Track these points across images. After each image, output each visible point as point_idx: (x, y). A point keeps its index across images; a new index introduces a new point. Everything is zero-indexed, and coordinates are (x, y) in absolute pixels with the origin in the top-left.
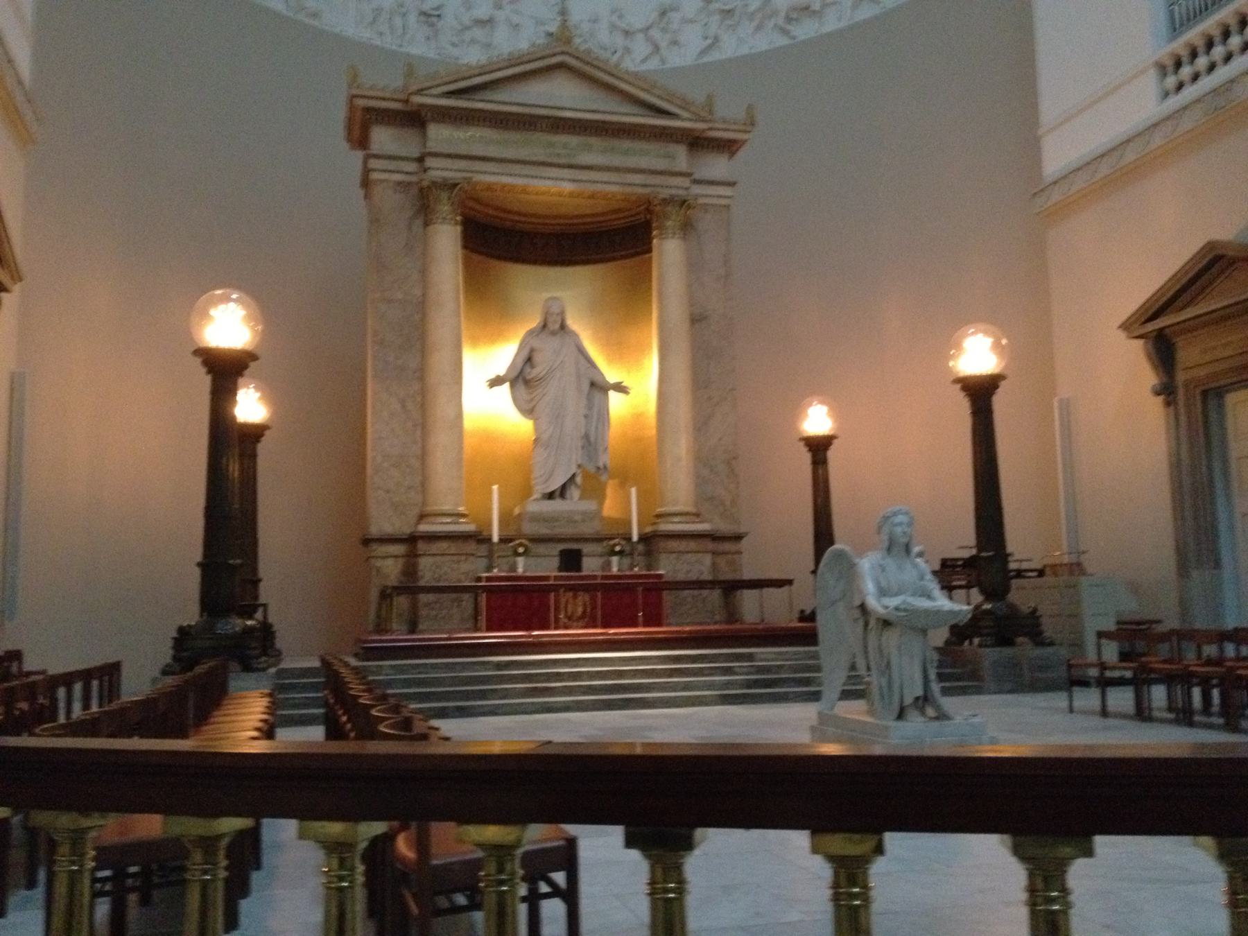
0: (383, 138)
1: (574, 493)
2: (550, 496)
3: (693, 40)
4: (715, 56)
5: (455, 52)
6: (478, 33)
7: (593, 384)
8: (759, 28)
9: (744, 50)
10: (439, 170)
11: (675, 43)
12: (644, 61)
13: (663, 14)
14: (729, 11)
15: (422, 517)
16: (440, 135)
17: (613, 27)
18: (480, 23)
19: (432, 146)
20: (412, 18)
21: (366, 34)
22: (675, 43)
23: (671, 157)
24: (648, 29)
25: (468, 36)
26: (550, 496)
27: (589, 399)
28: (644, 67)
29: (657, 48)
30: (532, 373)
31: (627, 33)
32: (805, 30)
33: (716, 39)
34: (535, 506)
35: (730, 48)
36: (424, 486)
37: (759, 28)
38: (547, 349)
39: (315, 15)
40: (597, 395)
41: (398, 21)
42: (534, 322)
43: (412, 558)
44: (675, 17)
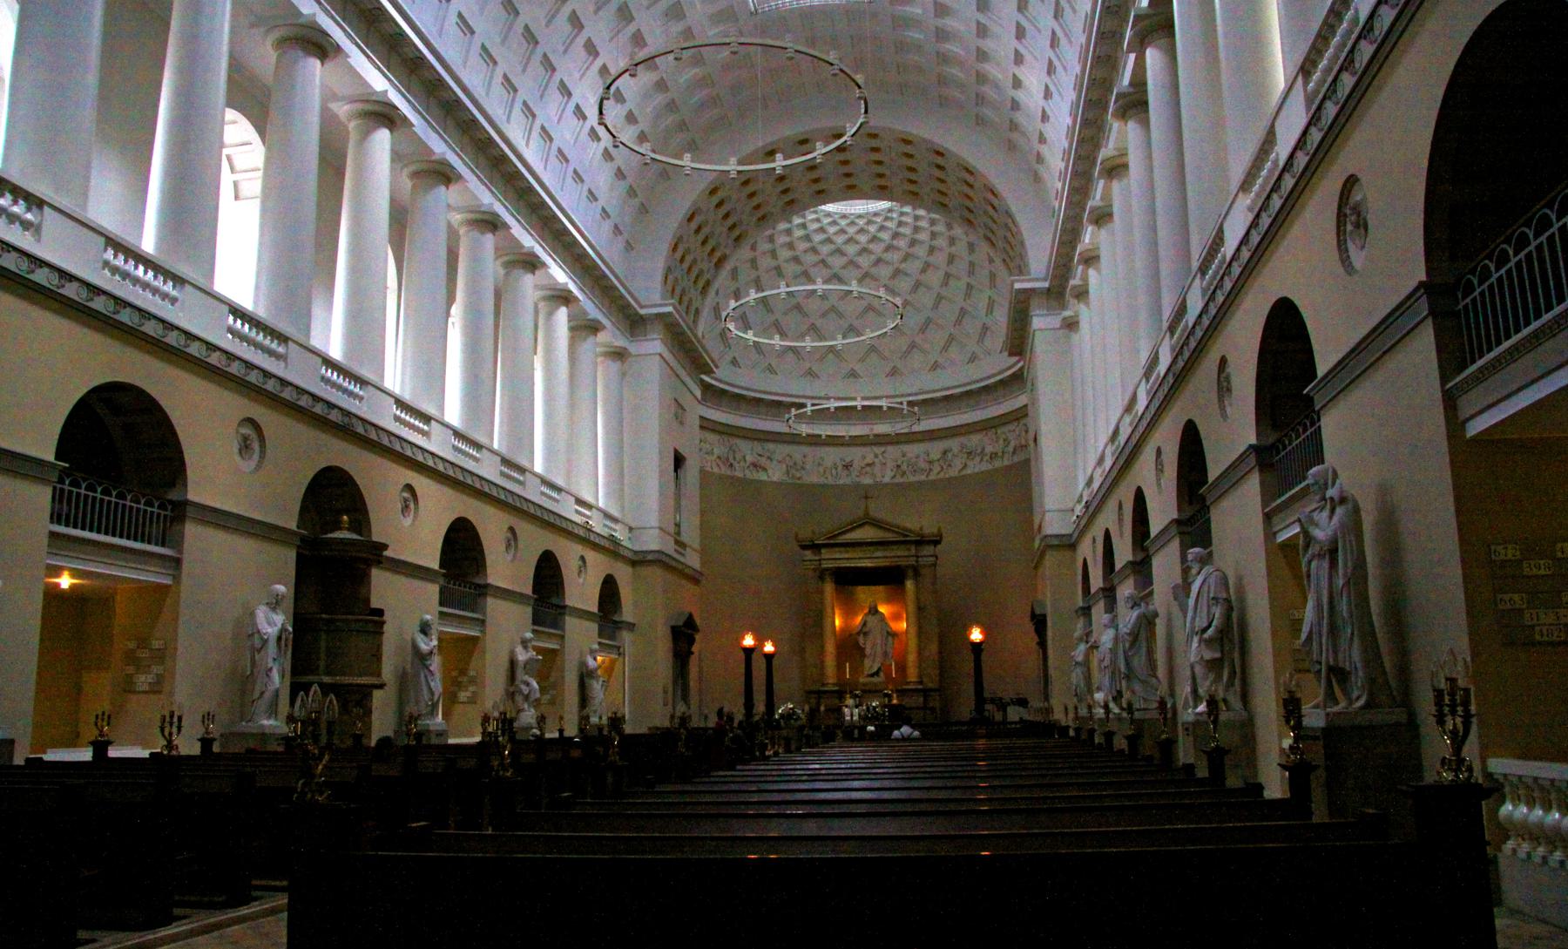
0: (808, 554)
1: (882, 674)
2: (872, 675)
3: (958, 464)
4: (964, 472)
5: (857, 479)
6: (868, 469)
7: (888, 632)
8: (982, 460)
9: (976, 470)
10: (825, 565)
11: (950, 465)
12: (938, 473)
13: (945, 453)
14: (970, 453)
15: (823, 685)
16: (825, 553)
17: (924, 460)
18: (868, 465)
19: (823, 556)
20: (840, 468)
21: (822, 480)
22: (950, 465)
23: (909, 550)
24: (938, 460)
25: (864, 470)
26: (872, 675)
27: (887, 638)
28: (939, 477)
29: (942, 467)
30: (865, 630)
31: (931, 462)
32: (998, 464)
33: (966, 465)
34: (862, 680)
35: (969, 471)
36: (822, 674)
37: (982, 460)
38: (872, 621)
39: (799, 479)
40: (890, 638)
41: (834, 471)
42: (866, 611)
43: (819, 698)
44: (950, 455)
